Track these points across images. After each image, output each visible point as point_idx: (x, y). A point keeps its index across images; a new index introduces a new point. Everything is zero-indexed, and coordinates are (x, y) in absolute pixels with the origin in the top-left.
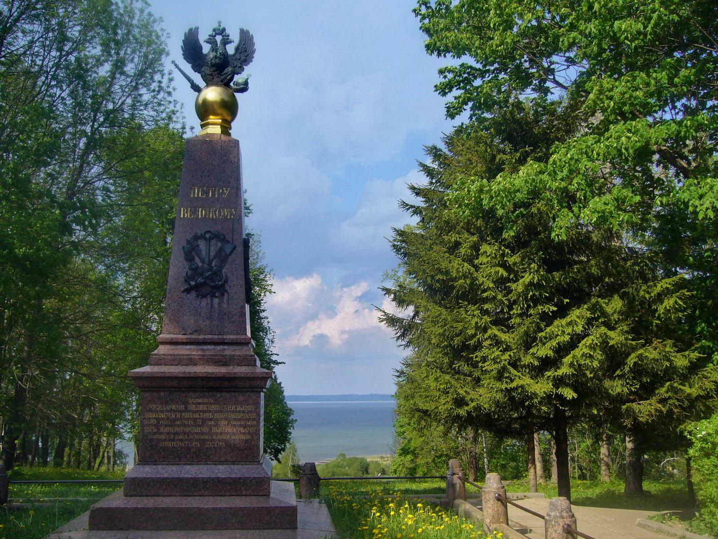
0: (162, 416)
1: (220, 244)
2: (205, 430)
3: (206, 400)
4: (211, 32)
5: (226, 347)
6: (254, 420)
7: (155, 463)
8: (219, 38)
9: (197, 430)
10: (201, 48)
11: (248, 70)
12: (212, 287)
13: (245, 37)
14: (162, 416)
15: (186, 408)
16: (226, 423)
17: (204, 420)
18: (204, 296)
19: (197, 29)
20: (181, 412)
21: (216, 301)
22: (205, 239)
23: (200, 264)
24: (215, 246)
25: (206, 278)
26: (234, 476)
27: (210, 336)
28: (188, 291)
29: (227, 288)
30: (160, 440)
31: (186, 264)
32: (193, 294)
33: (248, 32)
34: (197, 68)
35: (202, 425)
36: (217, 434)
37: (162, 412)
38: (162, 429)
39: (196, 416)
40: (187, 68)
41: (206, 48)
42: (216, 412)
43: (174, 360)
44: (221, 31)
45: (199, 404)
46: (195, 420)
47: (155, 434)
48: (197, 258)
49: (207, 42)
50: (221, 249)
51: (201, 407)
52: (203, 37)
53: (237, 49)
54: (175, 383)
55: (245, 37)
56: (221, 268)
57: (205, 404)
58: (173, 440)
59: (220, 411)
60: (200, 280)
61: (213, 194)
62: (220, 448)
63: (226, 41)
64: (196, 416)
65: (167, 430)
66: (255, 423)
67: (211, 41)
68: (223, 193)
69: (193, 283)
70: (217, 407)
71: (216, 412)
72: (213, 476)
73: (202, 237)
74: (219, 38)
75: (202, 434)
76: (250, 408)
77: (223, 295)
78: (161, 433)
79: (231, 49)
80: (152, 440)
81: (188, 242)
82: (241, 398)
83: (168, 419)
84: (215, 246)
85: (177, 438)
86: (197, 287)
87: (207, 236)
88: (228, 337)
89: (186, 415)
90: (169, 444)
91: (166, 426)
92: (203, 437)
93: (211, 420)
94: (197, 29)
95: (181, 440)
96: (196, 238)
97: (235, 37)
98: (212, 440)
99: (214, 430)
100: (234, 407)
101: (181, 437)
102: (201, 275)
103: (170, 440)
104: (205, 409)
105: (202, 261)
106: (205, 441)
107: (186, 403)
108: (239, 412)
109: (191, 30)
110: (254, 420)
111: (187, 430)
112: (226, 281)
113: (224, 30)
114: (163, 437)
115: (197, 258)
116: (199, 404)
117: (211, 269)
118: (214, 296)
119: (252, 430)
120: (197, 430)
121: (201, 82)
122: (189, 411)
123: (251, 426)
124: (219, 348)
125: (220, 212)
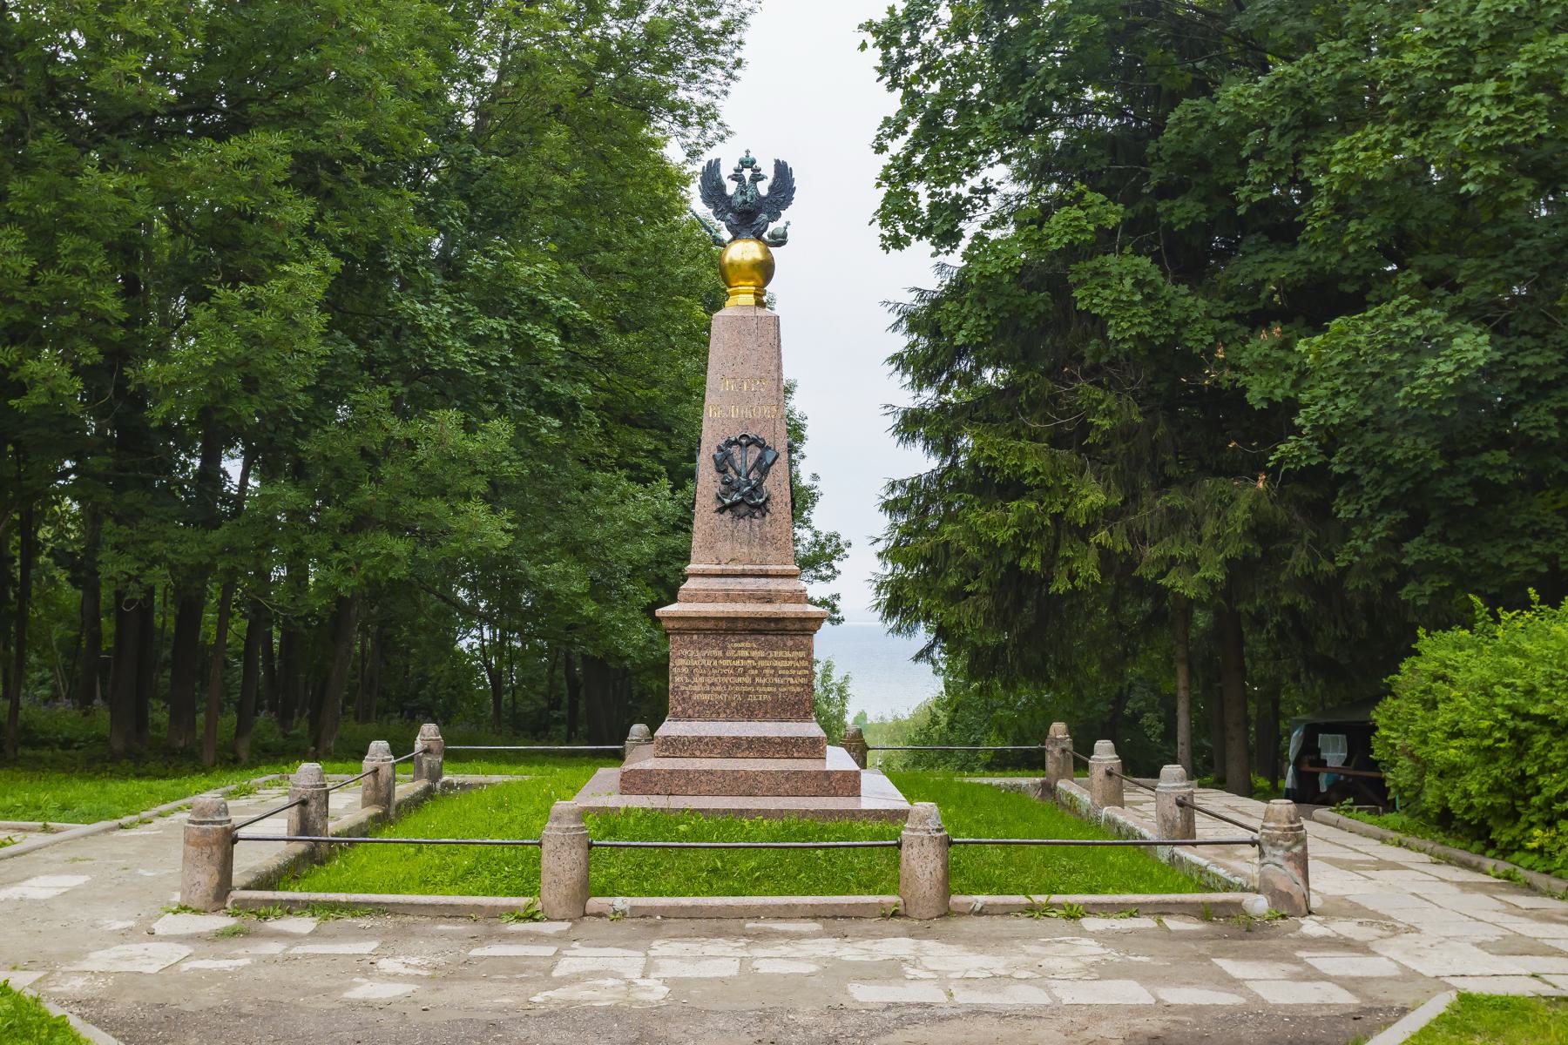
1: (759, 451)
2: (748, 680)
4: (736, 164)
5: (769, 580)
6: (806, 668)
7: (690, 718)
8: (747, 173)
9: (739, 680)
11: (786, 215)
12: (752, 506)
13: (782, 171)
18: (741, 517)
19: (718, 161)
21: (756, 521)
22: (741, 445)
23: (735, 477)
24: (754, 453)
25: (743, 495)
26: (782, 735)
27: (750, 567)
28: (721, 511)
29: (769, 506)
31: (719, 477)
32: (728, 515)
33: (785, 164)
36: (761, 685)
38: (695, 680)
39: (737, 663)
41: (731, 188)
43: (708, 596)
44: (747, 163)
46: (735, 668)
47: (687, 684)
48: (730, 469)
50: (760, 458)
51: (746, 653)
52: (726, 171)
53: (771, 188)
54: (710, 625)
55: (782, 171)
56: (760, 483)
58: (709, 692)
60: (737, 497)
61: (749, 388)
62: (766, 702)
63: (757, 177)
64: (737, 663)
67: (737, 177)
69: (727, 501)
70: (762, 654)
72: (758, 735)
73: (736, 442)
74: (747, 173)
75: (745, 684)
76: (802, 654)
77: (764, 515)
79: (763, 188)
81: (720, 449)
82: (790, 643)
84: (754, 453)
86: (732, 506)
87: (744, 441)
88: (772, 567)
89: (725, 663)
90: (706, 697)
92: (745, 689)
93: (754, 668)
94: (718, 161)
95: (719, 693)
96: (729, 443)
97: (769, 172)
100: (781, 654)
101: (718, 689)
102: (737, 490)
103: (705, 692)
105: (738, 473)
106: (749, 693)
107: (724, 649)
108: (788, 659)
110: (806, 668)
111: (725, 680)
112: (768, 499)
113: (753, 162)
115: (730, 469)
117: (749, 483)
118: (753, 516)
120: (739, 680)
124: (763, 580)
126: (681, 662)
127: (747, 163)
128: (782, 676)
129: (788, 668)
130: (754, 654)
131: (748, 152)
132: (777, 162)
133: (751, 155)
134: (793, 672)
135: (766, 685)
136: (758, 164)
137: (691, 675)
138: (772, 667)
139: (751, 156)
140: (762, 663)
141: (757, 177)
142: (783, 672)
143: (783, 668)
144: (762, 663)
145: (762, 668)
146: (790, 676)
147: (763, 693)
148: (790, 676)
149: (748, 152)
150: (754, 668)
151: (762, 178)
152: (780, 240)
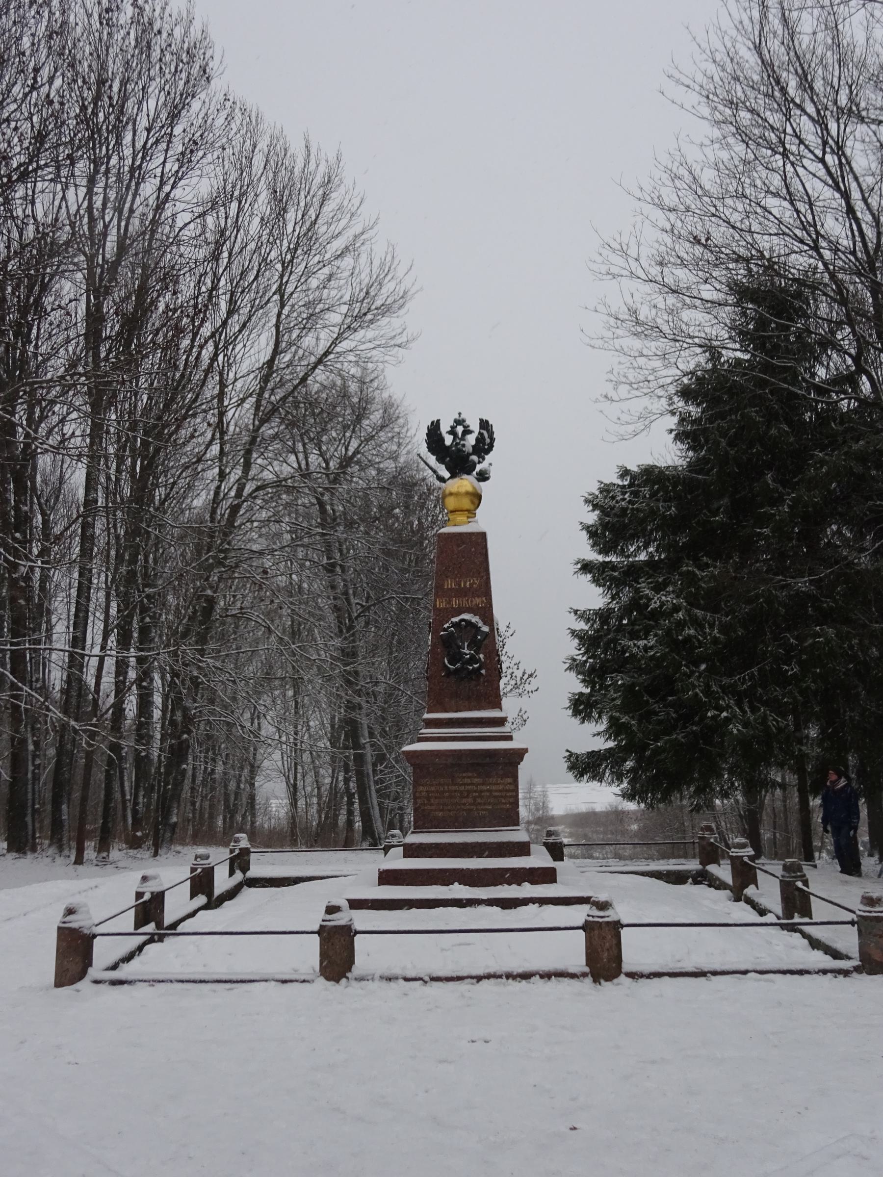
0: (433, 789)
2: (470, 800)
3: (470, 774)
4: (452, 423)
6: (512, 791)
8: (460, 429)
10: (443, 440)
13: (485, 425)
14: (433, 789)
15: (452, 781)
16: (488, 794)
17: (469, 792)
19: (438, 421)
20: (448, 785)
21: (473, 683)
30: (431, 810)
33: (487, 422)
34: (440, 460)
35: (467, 797)
36: (480, 804)
37: (432, 785)
39: (462, 788)
40: (432, 459)
41: (448, 440)
42: (479, 784)
45: (464, 777)
46: (461, 792)
47: (425, 805)
49: (450, 433)
52: (445, 428)
55: (485, 425)
57: (469, 777)
59: (483, 784)
63: (467, 431)
64: (462, 788)
65: (437, 801)
66: (514, 794)
67: (452, 432)
68: (474, 583)
71: (479, 784)
74: (460, 429)
76: (509, 780)
78: (431, 805)
79: (471, 440)
80: (424, 810)
83: (437, 792)
85: (445, 808)
91: (436, 798)
94: (438, 421)
95: (450, 811)
97: (475, 427)
98: (477, 810)
99: (479, 800)
101: (449, 807)
104: (469, 781)
109: (433, 423)
110: (512, 791)
113: (464, 421)
114: (433, 808)
116: (464, 777)
119: (511, 800)
121: (446, 474)
122: (456, 785)
123: (511, 797)
125: (472, 601)
126: (421, 788)
127: (459, 422)
128: (495, 797)
129: (500, 791)
130: (476, 780)
131: (460, 414)
132: (481, 420)
133: (462, 416)
134: (504, 794)
135: (485, 804)
136: (468, 422)
137: (428, 798)
138: (488, 791)
139: (462, 416)
140: (480, 787)
141: (467, 431)
142: (496, 794)
143: (496, 791)
144: (480, 787)
145: (481, 791)
146: (502, 797)
147: (483, 810)
148: (502, 797)
149: (460, 414)
150: (475, 792)
151: (470, 432)
152: (483, 477)
